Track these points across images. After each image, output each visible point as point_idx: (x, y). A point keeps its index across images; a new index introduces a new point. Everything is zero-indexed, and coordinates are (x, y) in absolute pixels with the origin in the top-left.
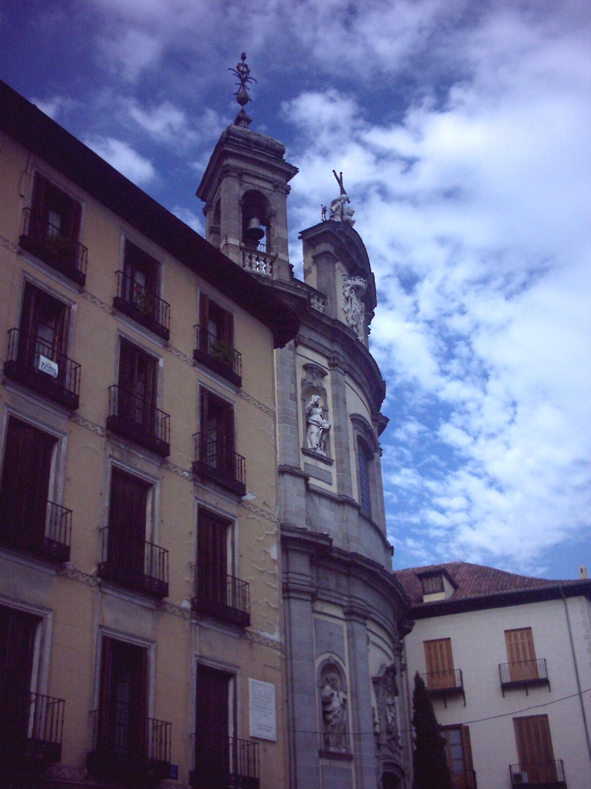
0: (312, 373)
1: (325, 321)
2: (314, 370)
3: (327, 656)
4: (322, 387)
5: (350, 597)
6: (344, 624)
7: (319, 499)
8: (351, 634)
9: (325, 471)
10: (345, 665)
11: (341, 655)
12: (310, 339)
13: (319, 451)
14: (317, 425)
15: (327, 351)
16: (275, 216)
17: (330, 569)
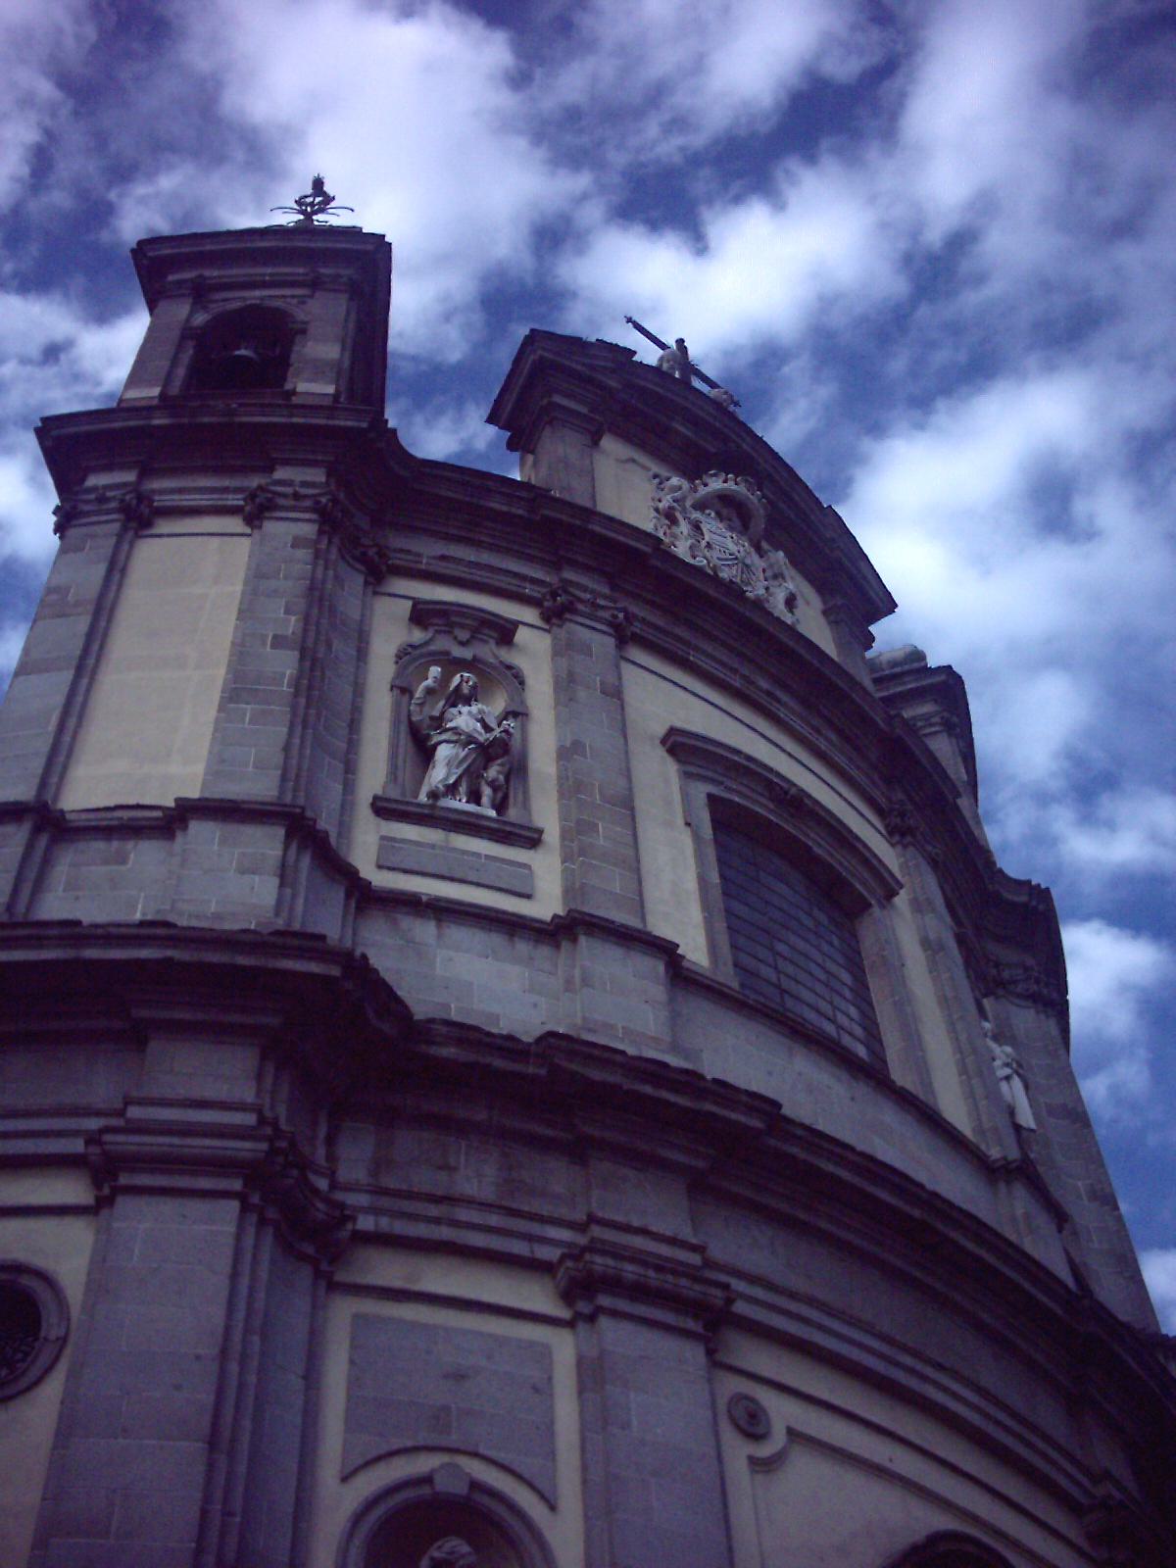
0: (450, 632)
1: (496, 505)
2: (454, 619)
3: (424, 1464)
4: (501, 662)
5: (581, 1227)
6: (564, 1347)
7: (439, 927)
8: (592, 1374)
10: (553, 1508)
11: (528, 1465)
12: (443, 558)
13: (460, 803)
14: (455, 738)
15: (528, 585)
16: (304, 332)
17: (462, 1129)
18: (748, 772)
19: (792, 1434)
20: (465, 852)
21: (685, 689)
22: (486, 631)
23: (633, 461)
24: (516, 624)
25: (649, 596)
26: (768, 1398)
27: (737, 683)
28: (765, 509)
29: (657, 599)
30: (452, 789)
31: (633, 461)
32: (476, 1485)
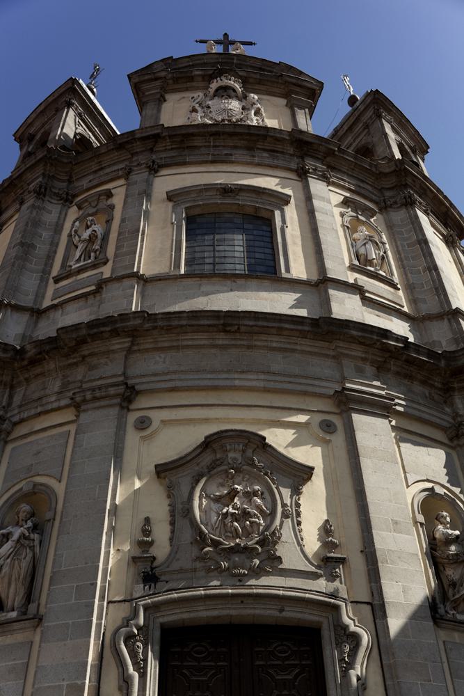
2: (90, 200)
9: (88, 277)
12: (90, 181)
18: (207, 190)
19: (163, 421)
20: (81, 279)
21: (185, 173)
22: (102, 197)
23: (184, 98)
24: (110, 189)
25: (170, 147)
26: (150, 414)
27: (210, 158)
28: (239, 82)
29: (173, 146)
30: (78, 261)
31: (184, 98)
32: (35, 485)
